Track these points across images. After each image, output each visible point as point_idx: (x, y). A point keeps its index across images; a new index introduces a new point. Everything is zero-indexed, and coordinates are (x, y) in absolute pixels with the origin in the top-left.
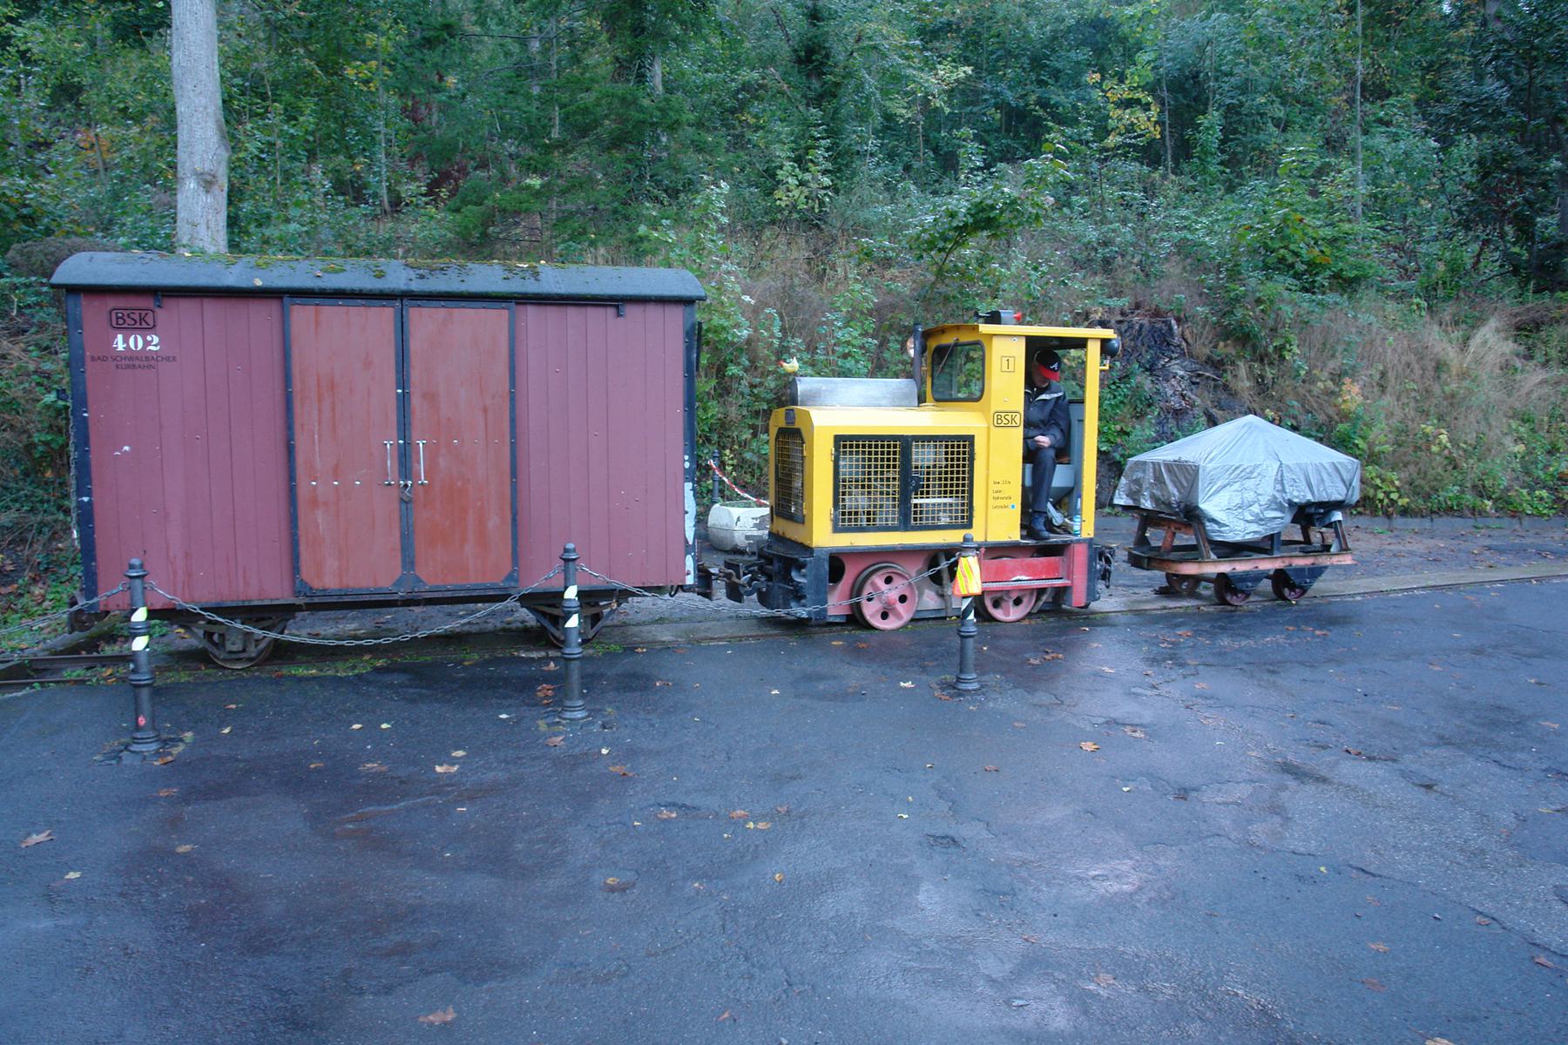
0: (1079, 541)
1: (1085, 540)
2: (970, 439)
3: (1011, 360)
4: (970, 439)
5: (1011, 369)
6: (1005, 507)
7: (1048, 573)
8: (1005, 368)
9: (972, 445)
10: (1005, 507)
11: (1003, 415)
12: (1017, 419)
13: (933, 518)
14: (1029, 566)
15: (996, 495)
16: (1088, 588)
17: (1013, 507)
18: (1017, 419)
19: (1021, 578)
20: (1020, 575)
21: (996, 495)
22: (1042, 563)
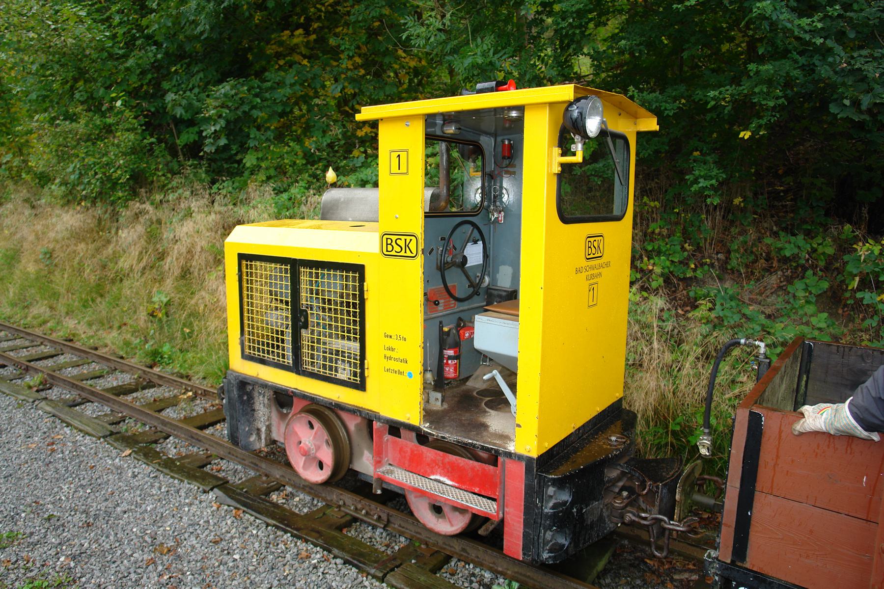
0: (509, 455)
1: (520, 457)
2: (359, 269)
3: (403, 155)
4: (359, 269)
5: (403, 169)
6: (401, 373)
7: (482, 486)
8: (395, 169)
9: (362, 279)
10: (401, 373)
11: (394, 238)
12: (413, 246)
13: (331, 368)
14: (452, 465)
15: (389, 353)
16: (526, 535)
17: (410, 375)
18: (413, 246)
19: (442, 479)
20: (441, 475)
21: (389, 353)
22: (473, 469)
